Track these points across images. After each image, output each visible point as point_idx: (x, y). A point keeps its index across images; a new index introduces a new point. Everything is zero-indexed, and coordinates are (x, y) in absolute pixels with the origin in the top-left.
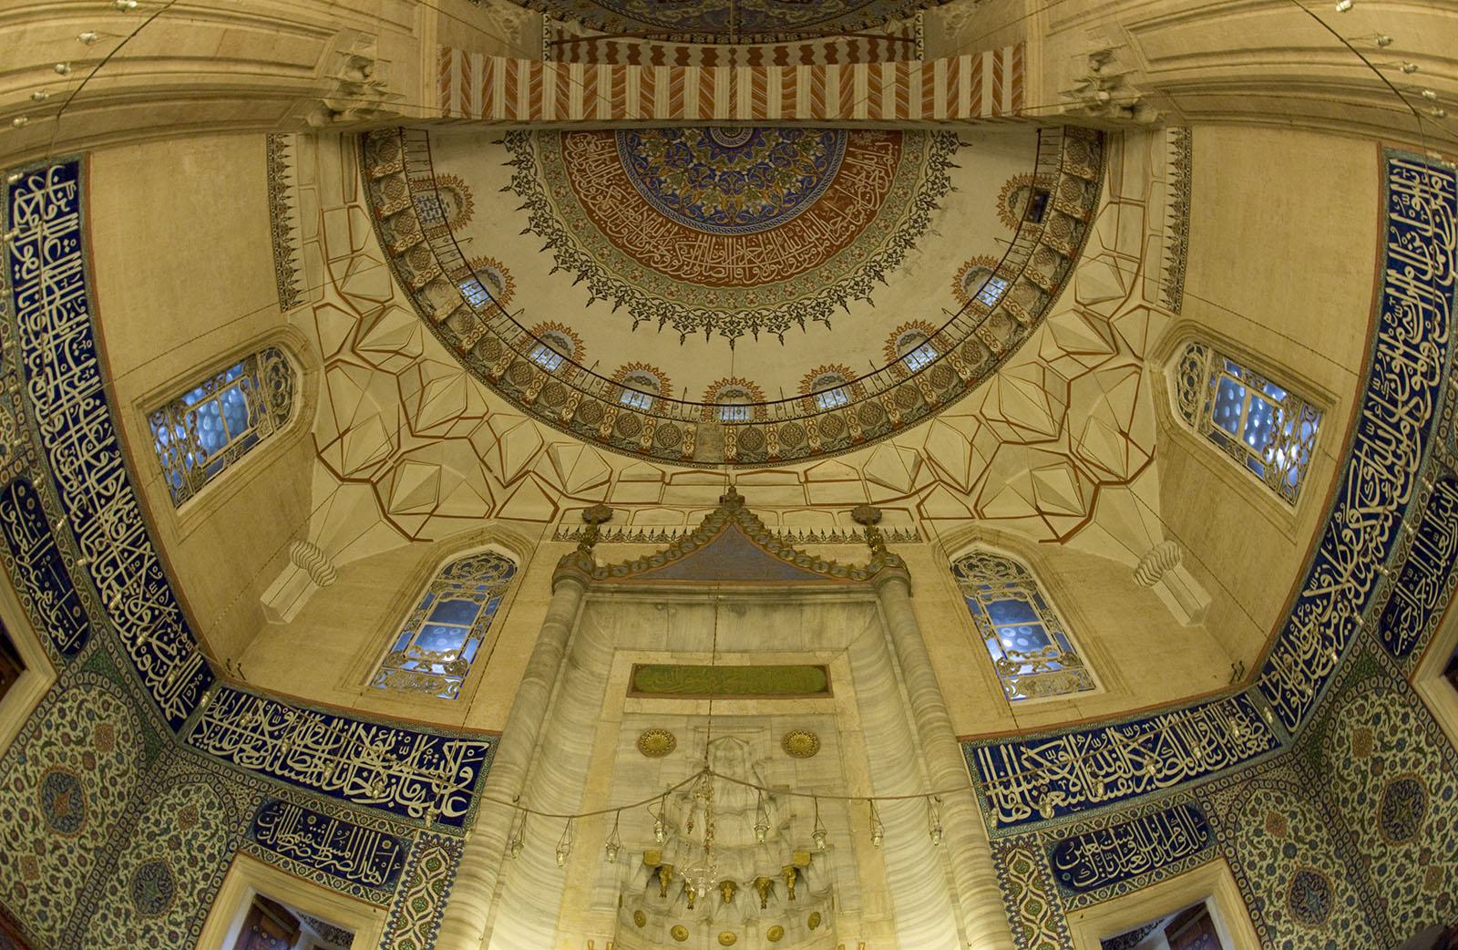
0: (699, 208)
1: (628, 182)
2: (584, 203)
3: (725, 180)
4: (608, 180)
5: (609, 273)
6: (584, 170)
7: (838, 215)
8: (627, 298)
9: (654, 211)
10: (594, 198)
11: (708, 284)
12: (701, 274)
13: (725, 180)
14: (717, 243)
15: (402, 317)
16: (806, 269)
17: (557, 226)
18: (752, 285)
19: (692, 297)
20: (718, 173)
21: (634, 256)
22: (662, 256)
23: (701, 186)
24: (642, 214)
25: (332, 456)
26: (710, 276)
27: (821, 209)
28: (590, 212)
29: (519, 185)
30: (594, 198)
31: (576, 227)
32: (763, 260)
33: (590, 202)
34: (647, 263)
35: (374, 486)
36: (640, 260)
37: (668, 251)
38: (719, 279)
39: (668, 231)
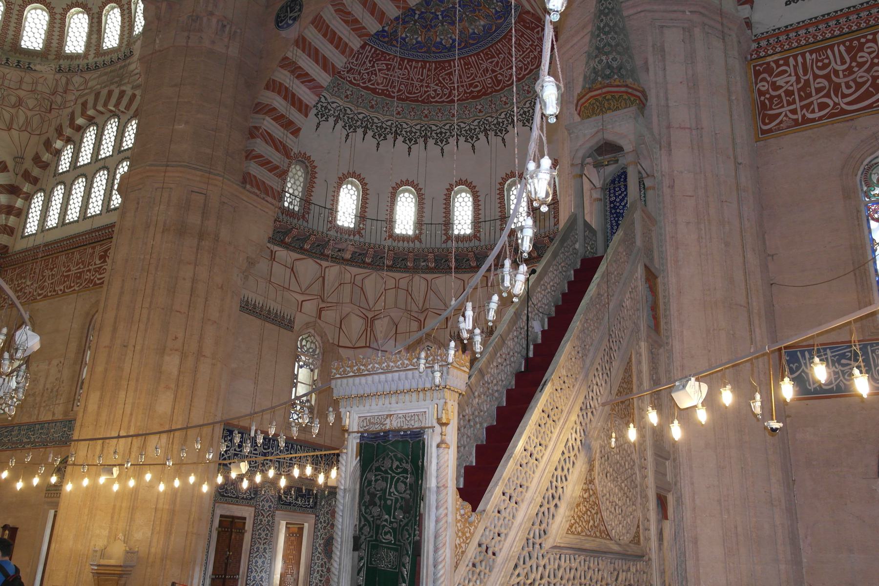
0: (441, 43)
1: (383, 53)
2: (366, 88)
3: (446, 16)
4: (370, 62)
5: (410, 123)
6: (351, 69)
7: (538, 27)
8: (429, 134)
9: (412, 61)
10: (370, 80)
11: (474, 98)
12: (466, 92)
13: (446, 16)
14: (465, 64)
15: (333, 271)
16: (531, 71)
17: (361, 116)
18: (502, 89)
19: (467, 112)
20: (439, 13)
21: (417, 101)
22: (435, 91)
23: (431, 27)
24: (406, 68)
25: (344, 342)
26: (472, 92)
27: (524, 21)
28: (374, 91)
29: (322, 115)
30: (370, 80)
31: (372, 107)
32: (501, 68)
33: (369, 85)
34: (427, 101)
35: (369, 347)
36: (423, 102)
37: (437, 85)
38: (479, 91)
39: (429, 70)
